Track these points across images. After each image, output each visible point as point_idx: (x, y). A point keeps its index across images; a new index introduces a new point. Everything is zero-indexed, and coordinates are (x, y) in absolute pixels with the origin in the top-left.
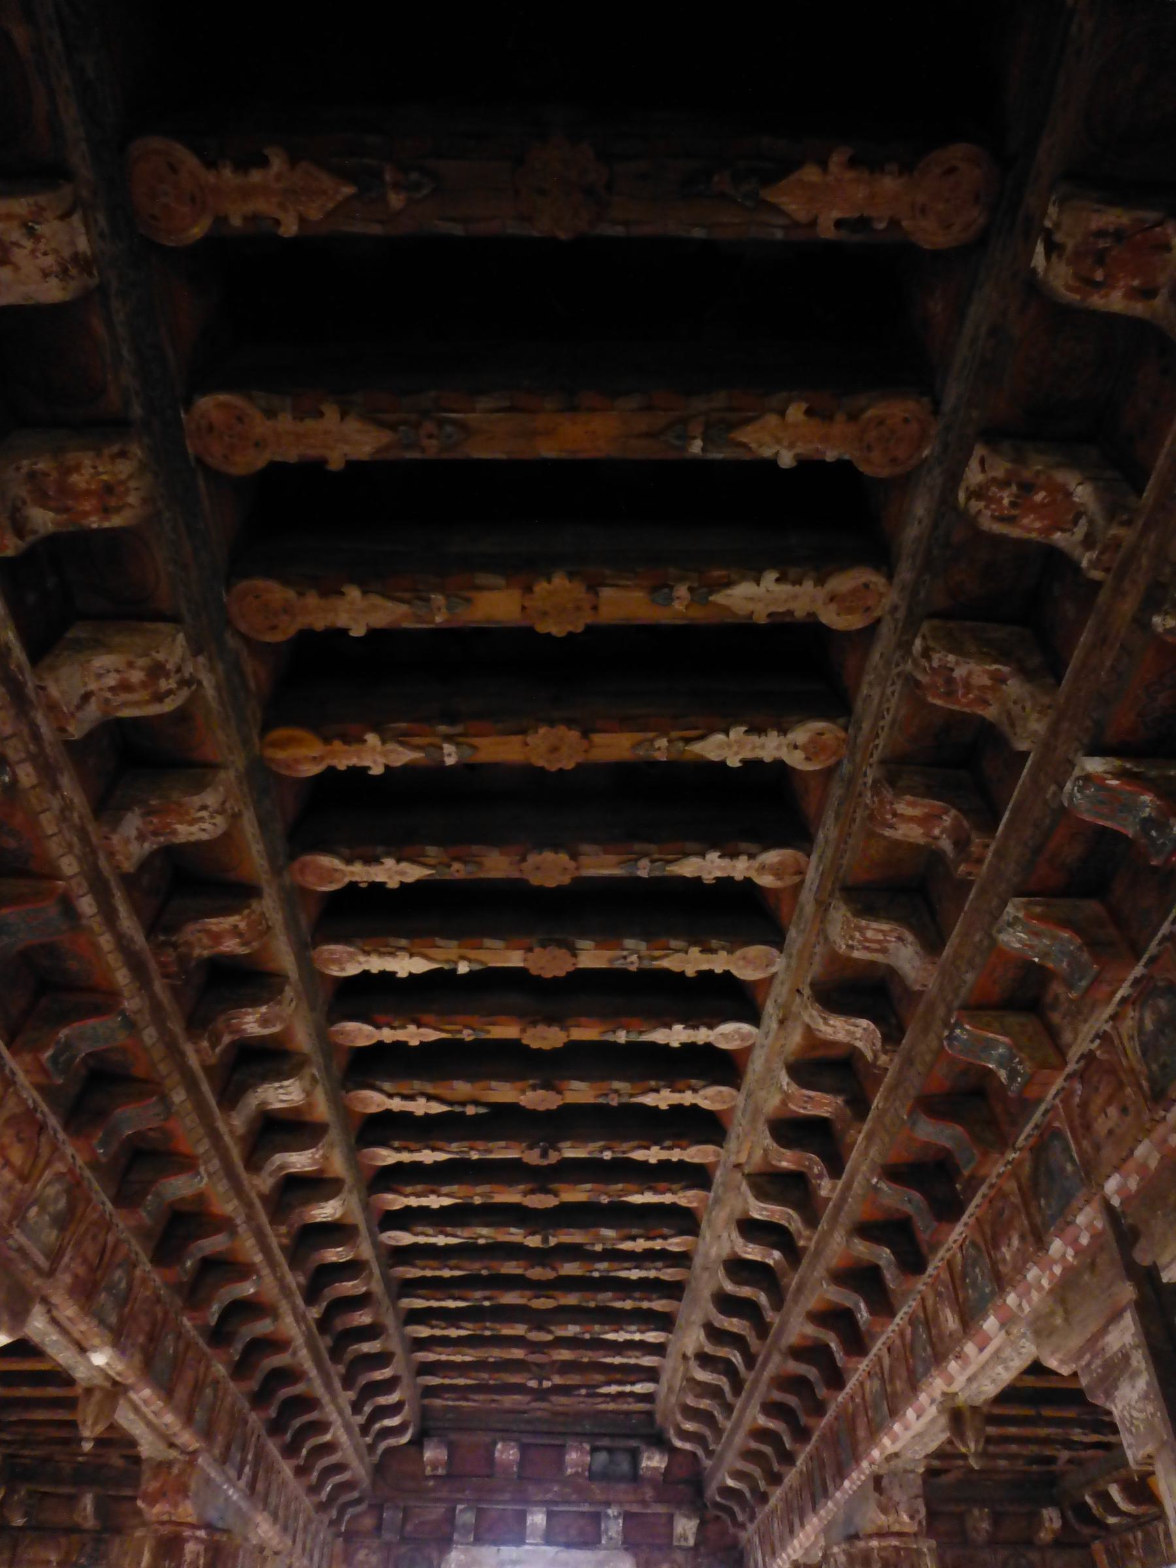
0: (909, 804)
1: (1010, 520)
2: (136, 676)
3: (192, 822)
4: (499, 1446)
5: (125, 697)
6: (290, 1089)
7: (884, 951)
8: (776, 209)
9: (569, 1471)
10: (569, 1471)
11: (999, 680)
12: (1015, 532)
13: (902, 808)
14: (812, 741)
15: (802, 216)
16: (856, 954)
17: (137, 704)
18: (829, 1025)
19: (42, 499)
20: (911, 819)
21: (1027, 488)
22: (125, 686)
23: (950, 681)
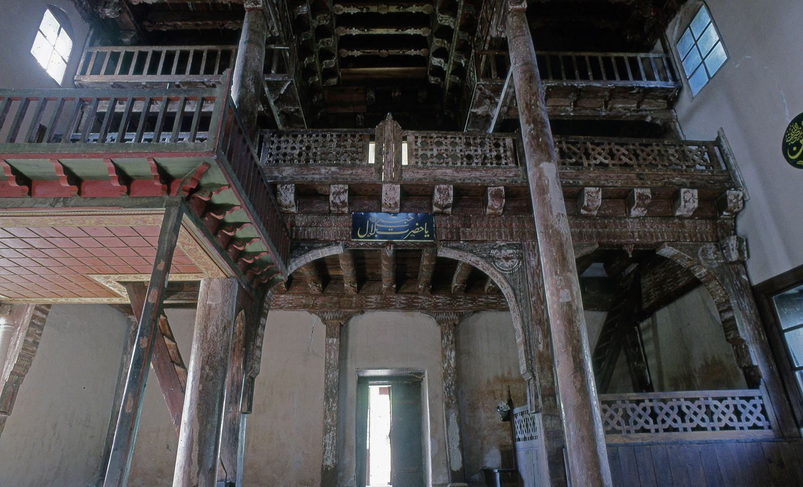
2: (444, 21)
11: (319, 22)
22: (446, 20)
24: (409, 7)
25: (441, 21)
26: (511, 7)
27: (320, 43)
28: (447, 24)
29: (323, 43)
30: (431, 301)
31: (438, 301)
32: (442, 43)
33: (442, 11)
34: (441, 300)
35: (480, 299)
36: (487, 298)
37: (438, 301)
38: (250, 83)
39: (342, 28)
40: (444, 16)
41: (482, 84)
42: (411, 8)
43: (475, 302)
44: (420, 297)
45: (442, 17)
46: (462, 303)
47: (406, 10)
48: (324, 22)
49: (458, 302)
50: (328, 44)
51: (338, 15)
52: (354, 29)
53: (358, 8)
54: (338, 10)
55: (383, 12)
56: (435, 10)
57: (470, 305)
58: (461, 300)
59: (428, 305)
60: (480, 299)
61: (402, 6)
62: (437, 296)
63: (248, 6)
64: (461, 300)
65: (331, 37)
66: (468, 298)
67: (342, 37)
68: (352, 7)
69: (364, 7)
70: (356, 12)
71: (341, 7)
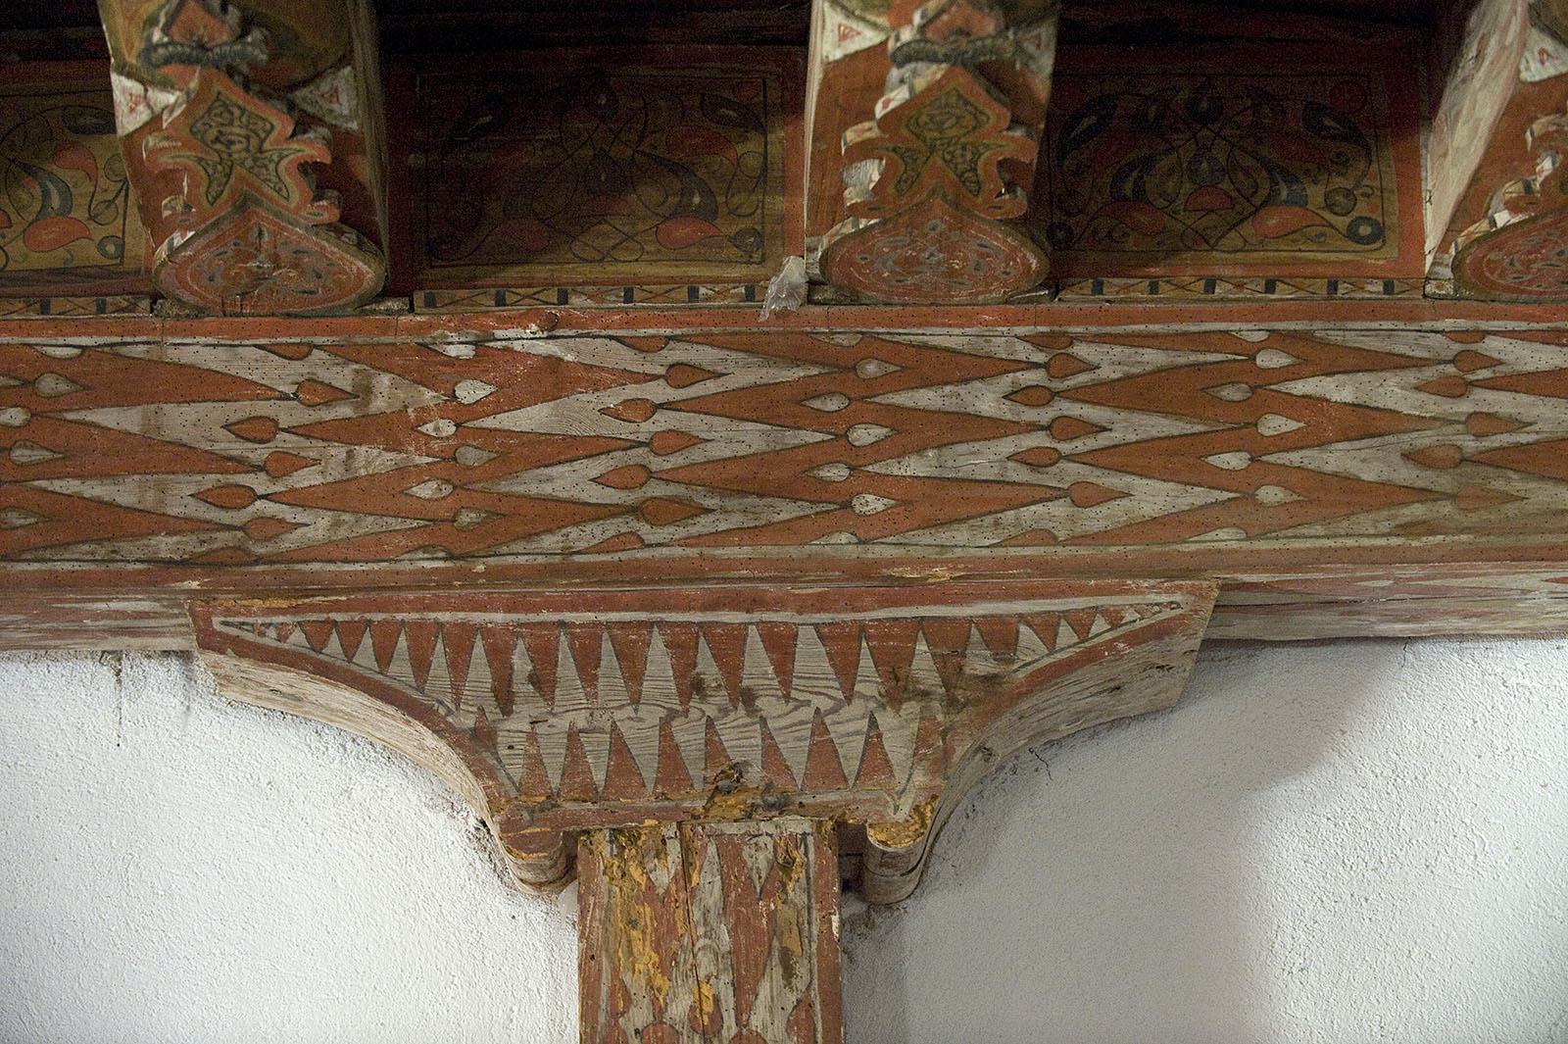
30: (392, 430)
31: (532, 418)
34: (579, 413)
35: (1340, 390)
36: (1465, 371)
37: (532, 418)
43: (1242, 432)
44: (199, 352)
46: (982, 460)
49: (912, 431)
57: (1153, 497)
58: (986, 399)
59: (332, 498)
60: (1340, 390)
62: (527, 340)
64: (986, 399)
66: (1109, 362)
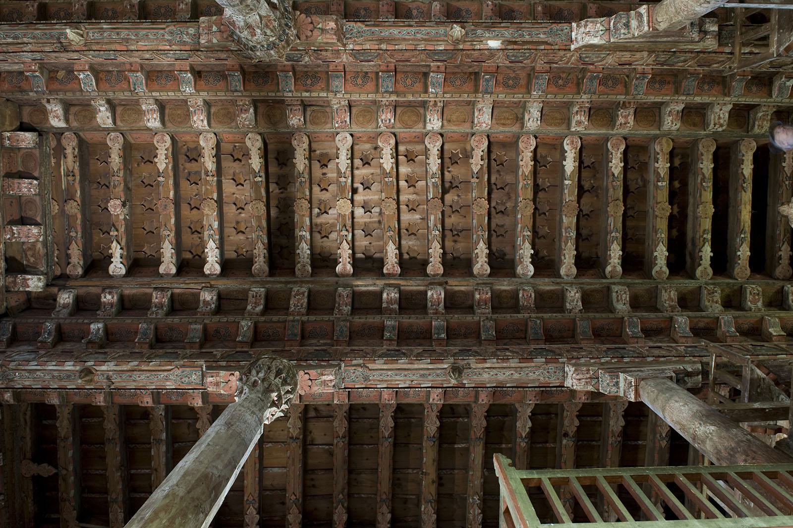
0: (674, 294)
1: (751, 293)
2: (722, 121)
3: (672, 121)
4: (35, 182)
5: (717, 117)
6: (535, 123)
7: (618, 301)
8: (783, 244)
9: (14, 228)
10: (14, 228)
12: (748, 295)
13: (672, 293)
14: (663, 272)
15: (782, 249)
16: (614, 294)
17: (715, 119)
18: (575, 293)
19: (764, 115)
20: (670, 295)
21: (758, 294)
22: (719, 118)
23: (713, 293)
24: (703, 174)
25: (721, 126)
26: (646, 28)
27: (753, 306)
28: (727, 115)
29: (754, 302)
32: (763, 119)
33: (704, 124)
38: (702, 428)
39: (737, 270)
40: (712, 123)
41: (778, 48)
42: (705, 171)
45: (715, 125)
47: (707, 176)
48: (717, 296)
50: (758, 294)
51: (714, 274)
52: (739, 253)
53: (704, 245)
54: (705, 271)
55: (711, 210)
56: (707, 136)
61: (702, 184)
63: (633, 396)
65: (746, 288)
67: (752, 271)
68: (700, 254)
69: (702, 236)
70: (709, 249)
71: (700, 268)
